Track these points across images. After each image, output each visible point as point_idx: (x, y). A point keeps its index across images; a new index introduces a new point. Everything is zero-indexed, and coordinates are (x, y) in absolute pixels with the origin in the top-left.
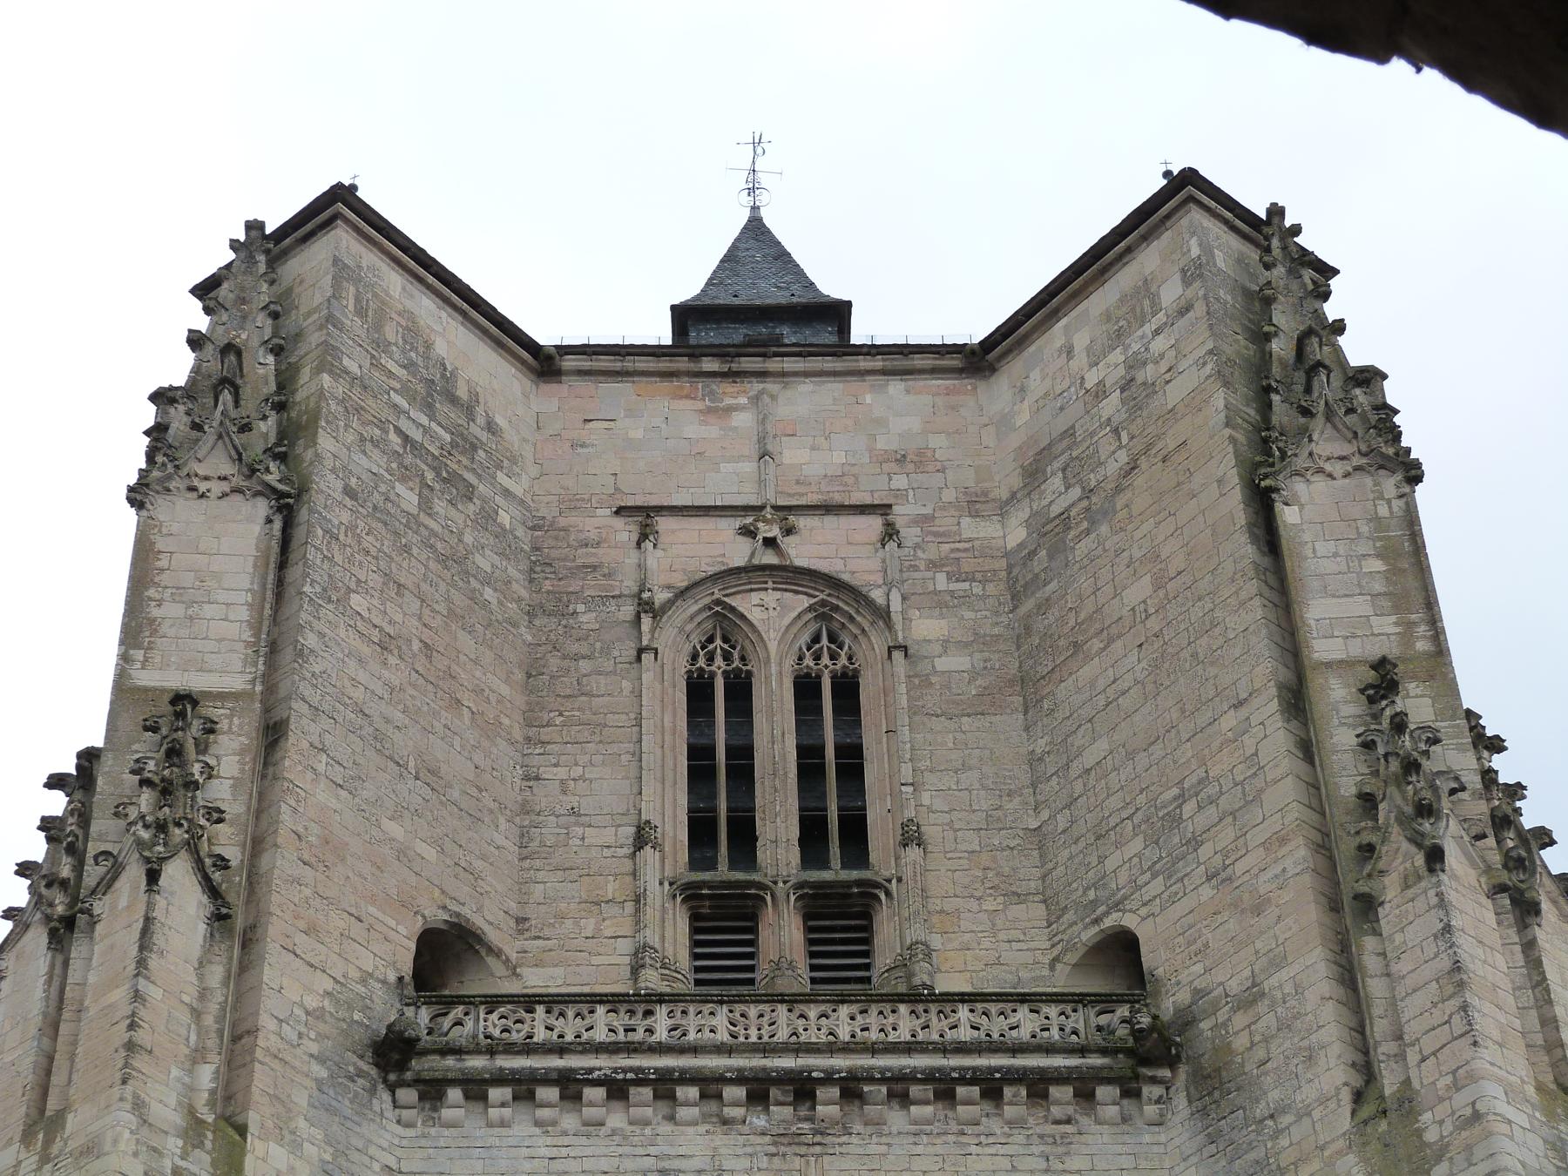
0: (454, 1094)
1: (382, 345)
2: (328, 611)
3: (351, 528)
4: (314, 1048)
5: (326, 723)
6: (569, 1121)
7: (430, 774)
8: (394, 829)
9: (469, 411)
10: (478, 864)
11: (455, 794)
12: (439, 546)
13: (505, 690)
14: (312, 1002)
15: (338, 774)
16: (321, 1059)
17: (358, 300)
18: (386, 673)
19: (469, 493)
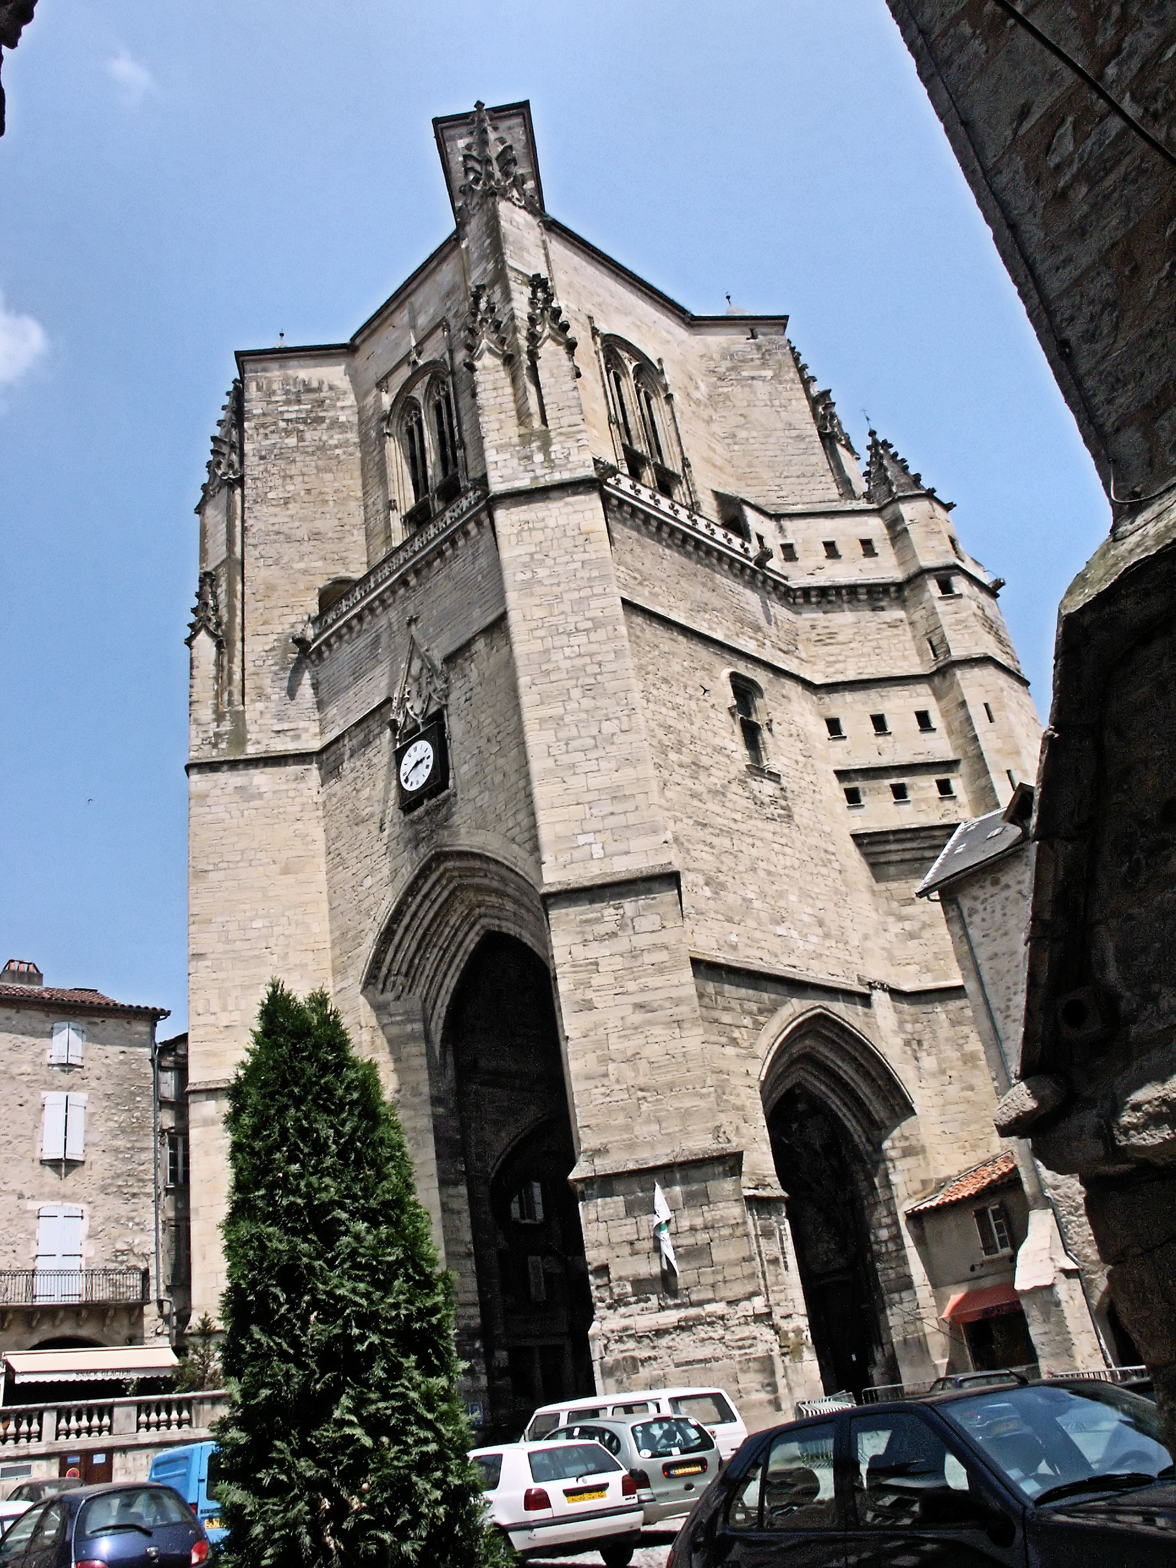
0: (323, 648)
1: (274, 393)
2: (257, 507)
3: (266, 470)
4: (271, 662)
5: (261, 547)
6: (354, 635)
7: (316, 536)
8: (301, 565)
9: (319, 389)
10: (344, 554)
11: (330, 535)
12: (310, 450)
13: (350, 482)
14: (267, 648)
15: (270, 562)
16: (275, 664)
17: (258, 385)
18: (289, 512)
19: (323, 419)
